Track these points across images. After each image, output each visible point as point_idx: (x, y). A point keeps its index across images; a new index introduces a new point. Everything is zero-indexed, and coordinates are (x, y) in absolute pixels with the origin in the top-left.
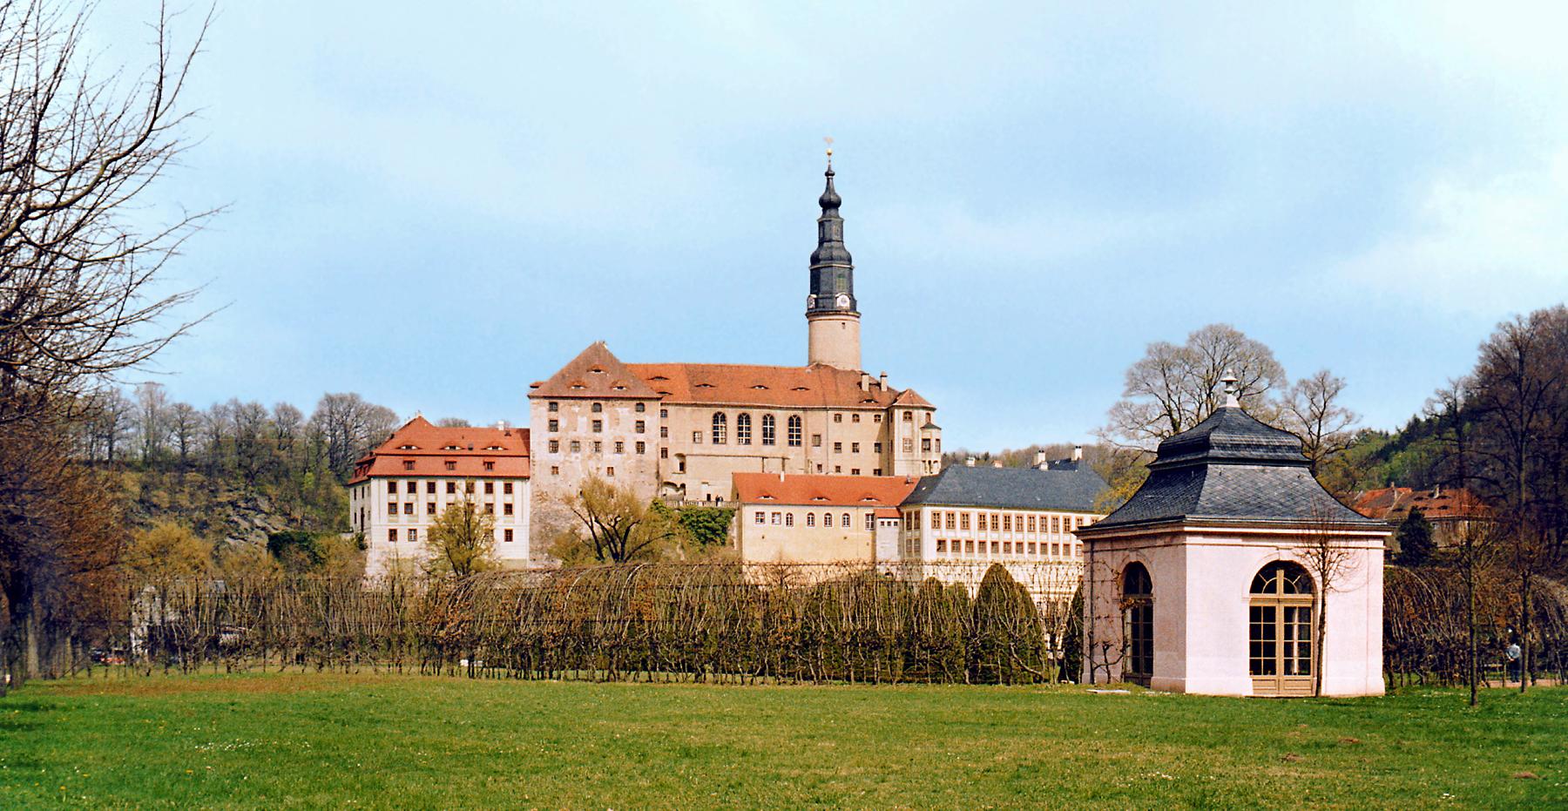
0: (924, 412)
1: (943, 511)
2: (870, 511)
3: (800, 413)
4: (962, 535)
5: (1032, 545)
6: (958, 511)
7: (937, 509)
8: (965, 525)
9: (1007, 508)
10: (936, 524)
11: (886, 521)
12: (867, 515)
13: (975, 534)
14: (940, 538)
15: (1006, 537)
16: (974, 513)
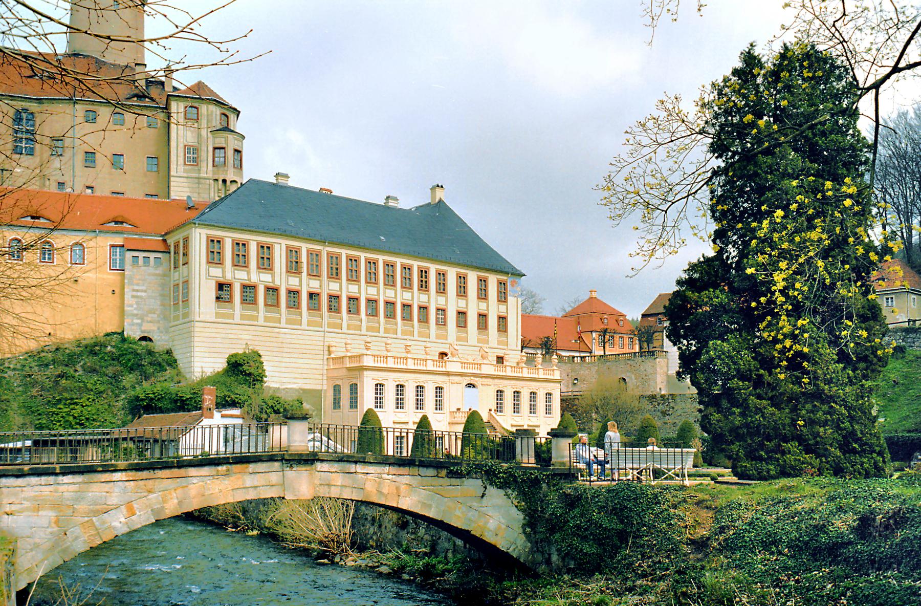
0: (216, 111)
1: (228, 238)
2: (119, 240)
3: (33, 107)
4: (260, 279)
5: (372, 302)
6: (253, 241)
7: (217, 233)
8: (266, 263)
9: (333, 243)
10: (215, 256)
11: (141, 255)
12: (112, 246)
13: (281, 278)
14: (222, 280)
15: (334, 287)
16: (280, 247)
